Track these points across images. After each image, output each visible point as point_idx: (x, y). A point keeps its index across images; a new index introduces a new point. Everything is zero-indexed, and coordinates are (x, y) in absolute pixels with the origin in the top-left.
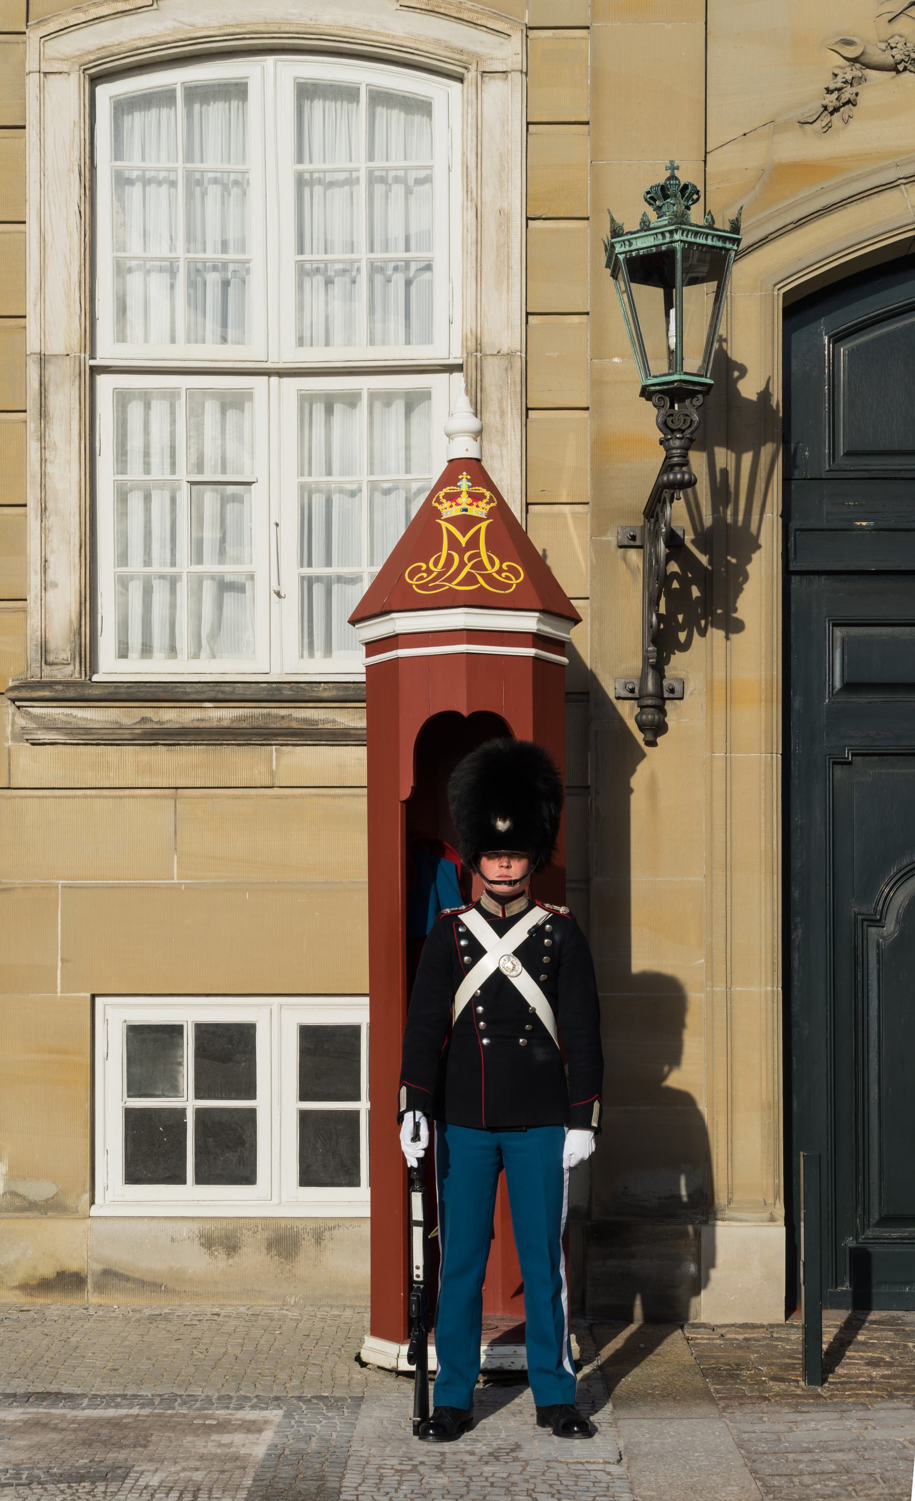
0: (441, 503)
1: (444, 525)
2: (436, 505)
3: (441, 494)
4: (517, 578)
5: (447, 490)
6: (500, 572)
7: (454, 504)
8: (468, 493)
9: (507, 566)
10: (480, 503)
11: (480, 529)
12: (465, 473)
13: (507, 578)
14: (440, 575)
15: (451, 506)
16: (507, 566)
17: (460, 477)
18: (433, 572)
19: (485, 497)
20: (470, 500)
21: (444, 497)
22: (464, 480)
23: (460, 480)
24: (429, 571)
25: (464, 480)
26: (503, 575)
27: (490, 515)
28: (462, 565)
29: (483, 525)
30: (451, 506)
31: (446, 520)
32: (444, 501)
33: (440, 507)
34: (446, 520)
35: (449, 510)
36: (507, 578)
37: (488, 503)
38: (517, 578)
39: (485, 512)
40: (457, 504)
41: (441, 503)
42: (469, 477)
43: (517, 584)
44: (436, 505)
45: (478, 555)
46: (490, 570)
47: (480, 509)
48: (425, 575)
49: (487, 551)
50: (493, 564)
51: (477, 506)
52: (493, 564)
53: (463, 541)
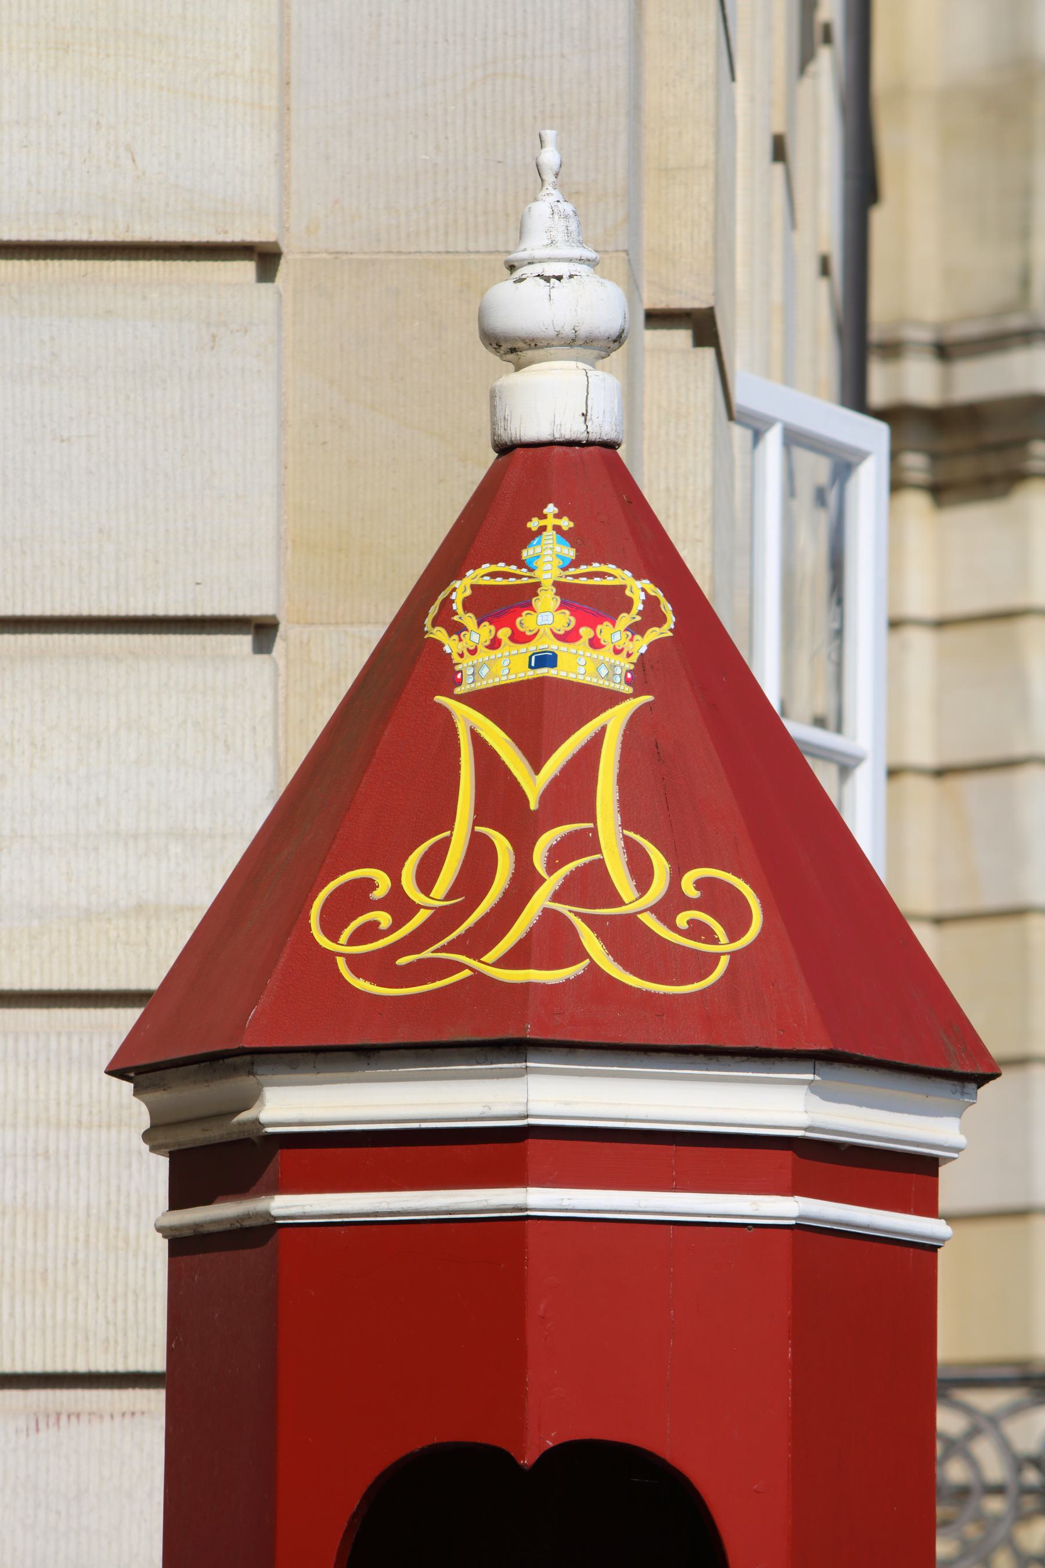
0: (456, 629)
1: (466, 718)
2: (439, 634)
3: (461, 590)
4: (736, 928)
5: (478, 576)
6: (665, 910)
7: (505, 633)
8: (561, 588)
9: (699, 884)
10: (606, 632)
12: (551, 509)
13: (697, 931)
14: (443, 921)
15: (495, 644)
16: (699, 884)
17: (534, 524)
19: (627, 605)
20: (564, 621)
22: (550, 535)
23: (531, 536)
24: (400, 906)
25: (550, 535)
26: (682, 920)
27: (643, 675)
28: (525, 882)
29: (614, 721)
30: (495, 644)
31: (478, 700)
32: (469, 620)
33: (451, 645)
34: (478, 700)
35: (488, 660)
36: (697, 931)
38: (736, 928)
39: (624, 664)
41: (456, 629)
42: (566, 523)
43: (733, 955)
44: (439, 634)
45: (589, 842)
46: (633, 901)
47: (605, 654)
48: (384, 919)
50: (642, 876)
51: (595, 643)
52: (642, 876)
53: (533, 786)
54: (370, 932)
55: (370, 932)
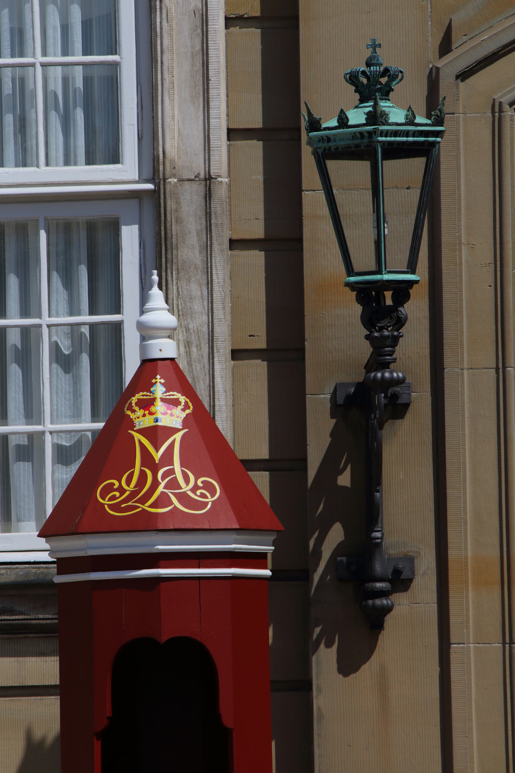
0: (134, 411)
1: (137, 436)
2: (129, 413)
3: (134, 400)
5: (139, 396)
7: (147, 412)
9: (202, 482)
11: (174, 441)
12: (158, 377)
14: (133, 494)
15: (144, 415)
16: (202, 482)
17: (154, 381)
18: (126, 491)
21: (137, 404)
24: (122, 491)
26: (198, 492)
27: (186, 422)
29: (178, 436)
30: (144, 415)
32: (137, 409)
33: (132, 416)
34: (139, 431)
37: (183, 410)
40: (151, 414)
41: (134, 411)
42: (163, 381)
44: (129, 413)
45: (172, 472)
47: (174, 418)
48: (117, 494)
49: (182, 466)
50: (187, 480)
51: (172, 415)
53: (157, 456)
54: (114, 498)
55: (114, 498)
